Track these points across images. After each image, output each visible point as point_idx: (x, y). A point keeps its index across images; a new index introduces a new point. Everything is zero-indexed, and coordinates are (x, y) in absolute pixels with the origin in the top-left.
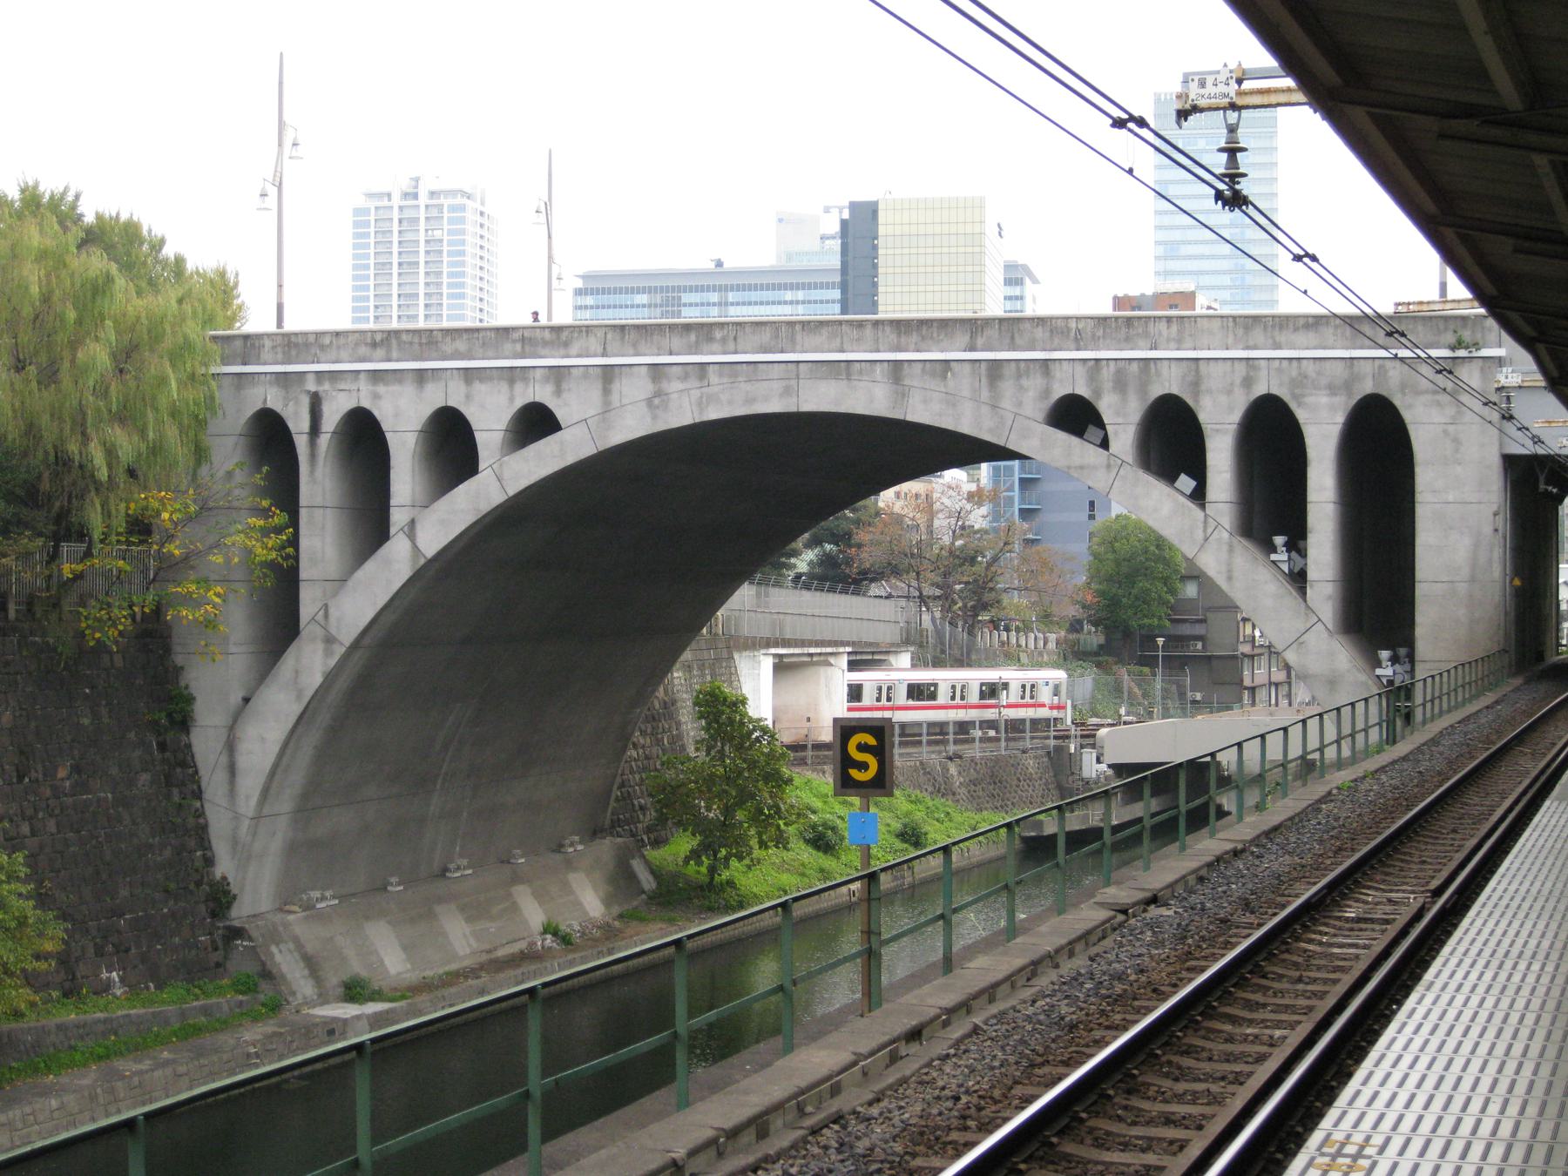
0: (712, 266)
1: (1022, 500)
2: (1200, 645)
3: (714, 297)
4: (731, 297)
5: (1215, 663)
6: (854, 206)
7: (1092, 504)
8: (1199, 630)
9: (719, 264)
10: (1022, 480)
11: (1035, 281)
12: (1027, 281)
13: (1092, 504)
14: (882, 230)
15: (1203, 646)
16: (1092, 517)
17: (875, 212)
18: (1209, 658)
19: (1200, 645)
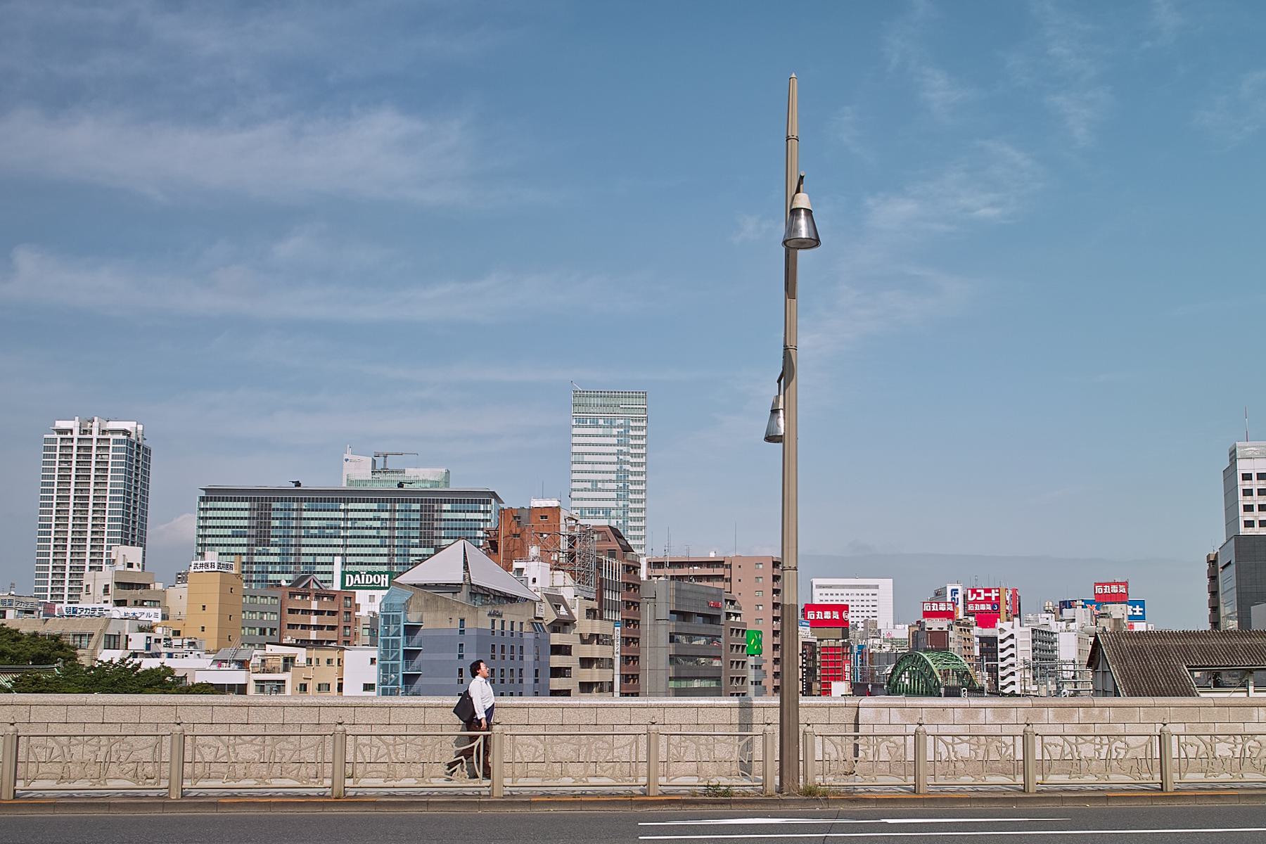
3: (295, 506)
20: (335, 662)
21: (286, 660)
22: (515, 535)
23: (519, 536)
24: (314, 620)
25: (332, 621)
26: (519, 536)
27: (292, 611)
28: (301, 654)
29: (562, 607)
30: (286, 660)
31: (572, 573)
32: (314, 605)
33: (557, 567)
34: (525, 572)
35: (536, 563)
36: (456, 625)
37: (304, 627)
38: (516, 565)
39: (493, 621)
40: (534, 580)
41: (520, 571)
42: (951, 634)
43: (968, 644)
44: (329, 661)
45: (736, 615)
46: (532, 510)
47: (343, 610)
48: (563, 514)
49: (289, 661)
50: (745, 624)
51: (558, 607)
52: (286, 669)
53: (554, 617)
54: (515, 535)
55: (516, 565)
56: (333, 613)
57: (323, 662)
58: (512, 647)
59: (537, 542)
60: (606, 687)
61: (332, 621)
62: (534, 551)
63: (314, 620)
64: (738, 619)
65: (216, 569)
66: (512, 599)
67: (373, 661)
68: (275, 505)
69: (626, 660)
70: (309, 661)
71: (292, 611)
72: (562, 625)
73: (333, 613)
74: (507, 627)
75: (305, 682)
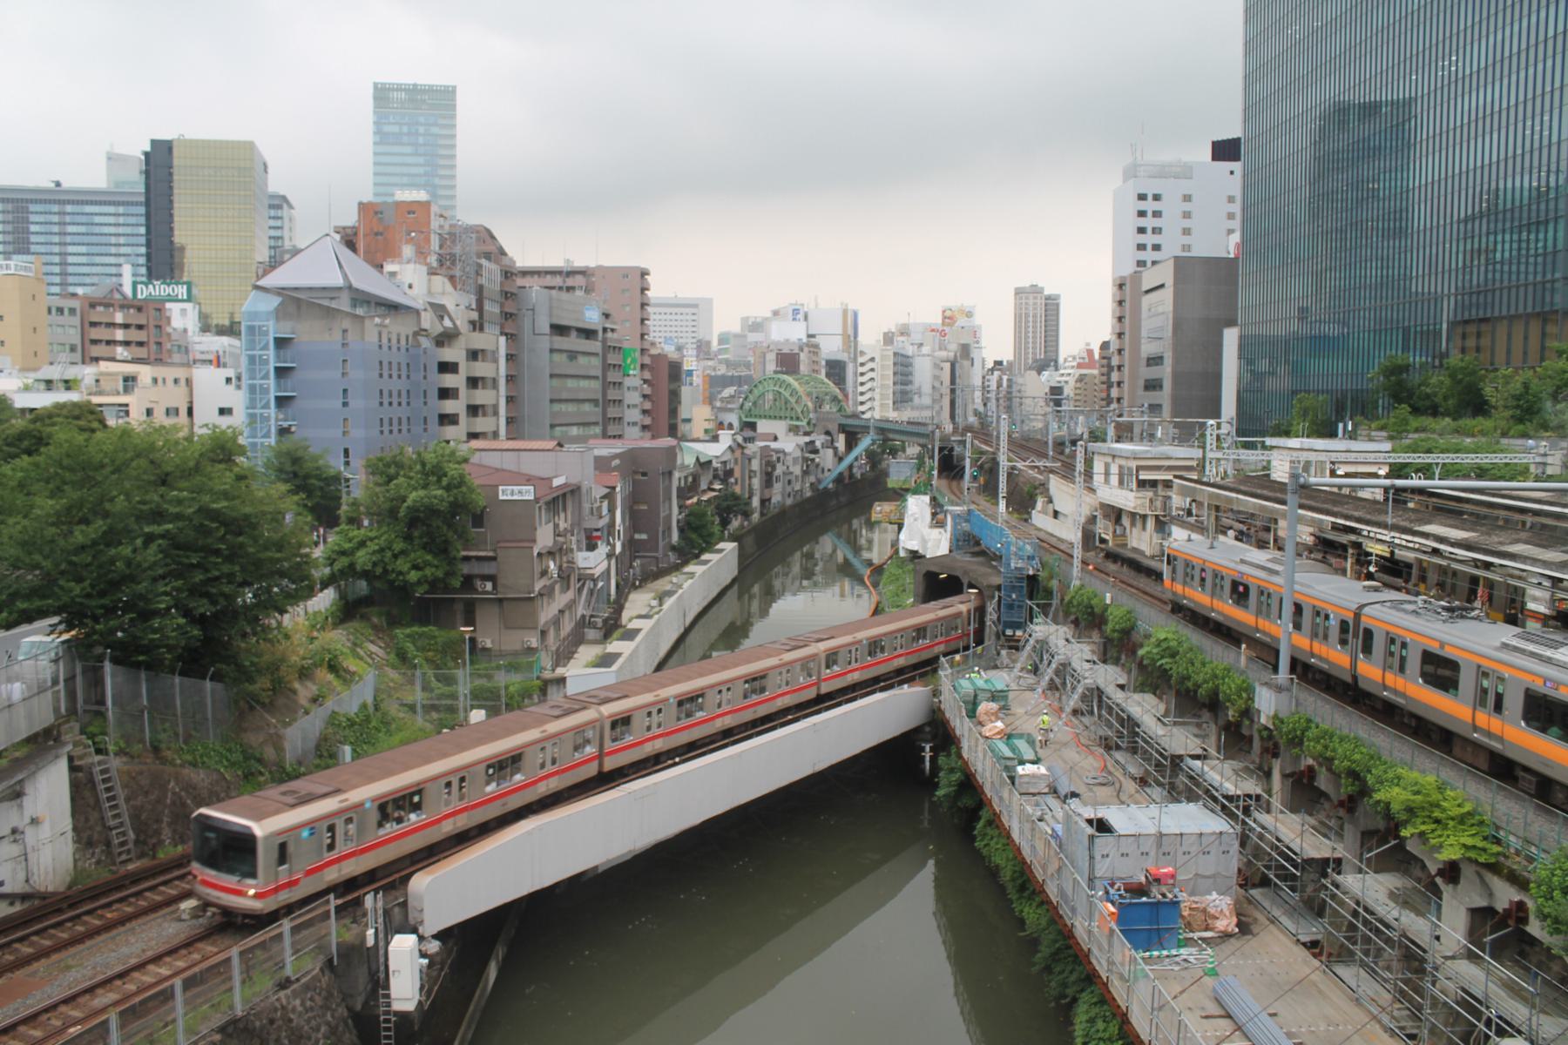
0: (53, 185)
1: (279, 387)
2: (489, 586)
3: (55, 208)
4: (69, 208)
5: (505, 603)
6: (154, 143)
7: (345, 391)
8: (487, 569)
9: (58, 184)
10: (277, 369)
11: (291, 207)
12: (285, 206)
13: (345, 391)
14: (176, 162)
15: (495, 587)
16: (345, 404)
17: (170, 149)
18: (500, 601)
19: (489, 586)
20: (183, 382)
21: (126, 379)
22: (376, 234)
23: (381, 234)
24: (120, 335)
25: (141, 336)
26: (381, 234)
27: (93, 324)
28: (145, 373)
29: (446, 319)
30: (126, 379)
31: (452, 278)
32: (119, 318)
33: (432, 272)
34: (399, 277)
35: (411, 266)
36: (338, 336)
37: (108, 343)
38: (389, 268)
39: (380, 334)
40: (410, 286)
41: (393, 274)
42: (803, 356)
43: (816, 368)
44: (176, 381)
45: (613, 330)
46: (399, 204)
47: (152, 323)
48: (434, 209)
49: (129, 381)
50: (620, 341)
51: (442, 318)
52: (127, 390)
53: (439, 329)
54: (376, 234)
55: (389, 268)
56: (140, 327)
57: (170, 382)
58: (390, 363)
59: (410, 241)
60: (490, 411)
61: (141, 336)
62: (408, 251)
63: (120, 335)
64: (615, 335)
65: (12, 272)
66: (393, 308)
67: (228, 380)
68: (33, 208)
69: (510, 379)
70: (155, 380)
71: (93, 324)
72: (444, 339)
73: (140, 327)
74: (394, 341)
75: (150, 405)
